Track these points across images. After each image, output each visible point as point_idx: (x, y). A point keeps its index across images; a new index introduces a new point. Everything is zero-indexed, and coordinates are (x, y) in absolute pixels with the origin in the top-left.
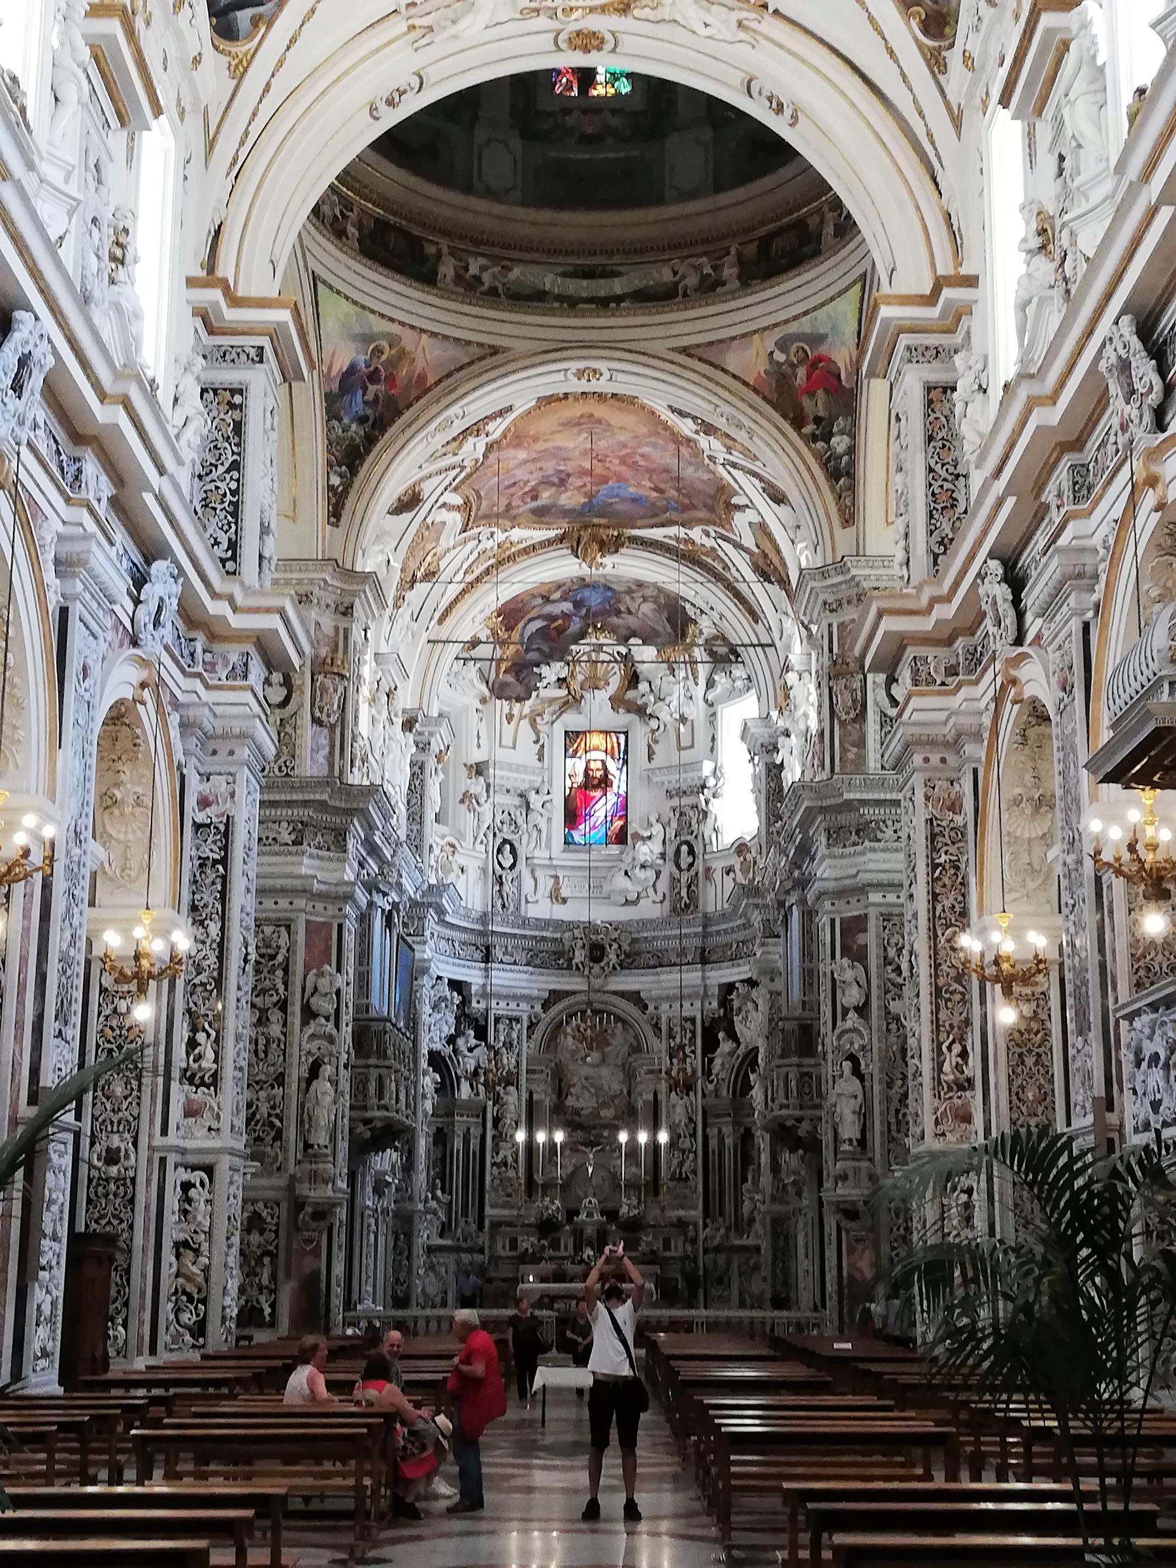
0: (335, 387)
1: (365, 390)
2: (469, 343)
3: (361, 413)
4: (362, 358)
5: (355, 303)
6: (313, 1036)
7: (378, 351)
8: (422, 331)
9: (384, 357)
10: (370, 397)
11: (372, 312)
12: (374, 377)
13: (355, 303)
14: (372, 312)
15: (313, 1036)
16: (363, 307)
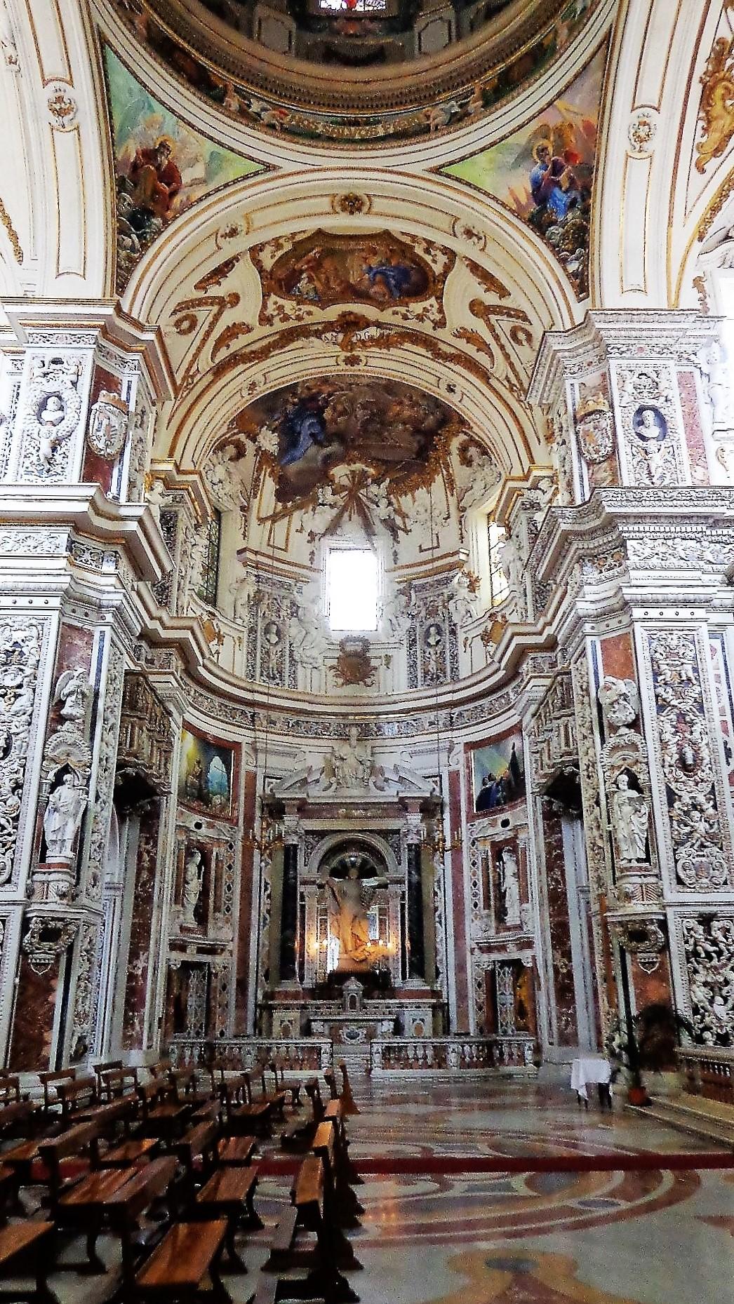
0: (534, 208)
1: (558, 184)
2: (585, 67)
3: (569, 200)
4: (537, 170)
5: (482, 150)
6: (615, 748)
7: (542, 151)
8: (550, 104)
9: (551, 150)
10: (566, 185)
11: (505, 137)
12: (557, 169)
13: (482, 150)
14: (505, 137)
15: (615, 748)
16: (492, 144)
